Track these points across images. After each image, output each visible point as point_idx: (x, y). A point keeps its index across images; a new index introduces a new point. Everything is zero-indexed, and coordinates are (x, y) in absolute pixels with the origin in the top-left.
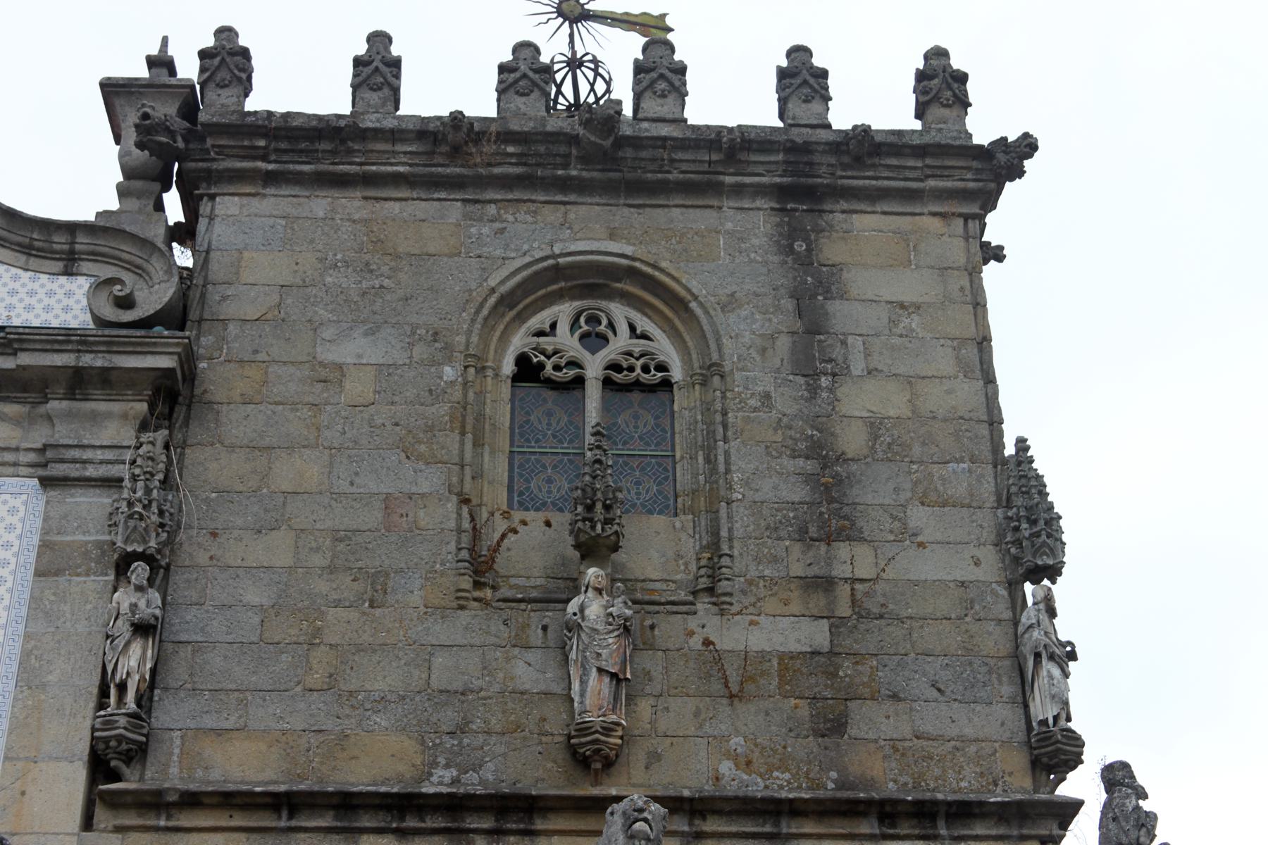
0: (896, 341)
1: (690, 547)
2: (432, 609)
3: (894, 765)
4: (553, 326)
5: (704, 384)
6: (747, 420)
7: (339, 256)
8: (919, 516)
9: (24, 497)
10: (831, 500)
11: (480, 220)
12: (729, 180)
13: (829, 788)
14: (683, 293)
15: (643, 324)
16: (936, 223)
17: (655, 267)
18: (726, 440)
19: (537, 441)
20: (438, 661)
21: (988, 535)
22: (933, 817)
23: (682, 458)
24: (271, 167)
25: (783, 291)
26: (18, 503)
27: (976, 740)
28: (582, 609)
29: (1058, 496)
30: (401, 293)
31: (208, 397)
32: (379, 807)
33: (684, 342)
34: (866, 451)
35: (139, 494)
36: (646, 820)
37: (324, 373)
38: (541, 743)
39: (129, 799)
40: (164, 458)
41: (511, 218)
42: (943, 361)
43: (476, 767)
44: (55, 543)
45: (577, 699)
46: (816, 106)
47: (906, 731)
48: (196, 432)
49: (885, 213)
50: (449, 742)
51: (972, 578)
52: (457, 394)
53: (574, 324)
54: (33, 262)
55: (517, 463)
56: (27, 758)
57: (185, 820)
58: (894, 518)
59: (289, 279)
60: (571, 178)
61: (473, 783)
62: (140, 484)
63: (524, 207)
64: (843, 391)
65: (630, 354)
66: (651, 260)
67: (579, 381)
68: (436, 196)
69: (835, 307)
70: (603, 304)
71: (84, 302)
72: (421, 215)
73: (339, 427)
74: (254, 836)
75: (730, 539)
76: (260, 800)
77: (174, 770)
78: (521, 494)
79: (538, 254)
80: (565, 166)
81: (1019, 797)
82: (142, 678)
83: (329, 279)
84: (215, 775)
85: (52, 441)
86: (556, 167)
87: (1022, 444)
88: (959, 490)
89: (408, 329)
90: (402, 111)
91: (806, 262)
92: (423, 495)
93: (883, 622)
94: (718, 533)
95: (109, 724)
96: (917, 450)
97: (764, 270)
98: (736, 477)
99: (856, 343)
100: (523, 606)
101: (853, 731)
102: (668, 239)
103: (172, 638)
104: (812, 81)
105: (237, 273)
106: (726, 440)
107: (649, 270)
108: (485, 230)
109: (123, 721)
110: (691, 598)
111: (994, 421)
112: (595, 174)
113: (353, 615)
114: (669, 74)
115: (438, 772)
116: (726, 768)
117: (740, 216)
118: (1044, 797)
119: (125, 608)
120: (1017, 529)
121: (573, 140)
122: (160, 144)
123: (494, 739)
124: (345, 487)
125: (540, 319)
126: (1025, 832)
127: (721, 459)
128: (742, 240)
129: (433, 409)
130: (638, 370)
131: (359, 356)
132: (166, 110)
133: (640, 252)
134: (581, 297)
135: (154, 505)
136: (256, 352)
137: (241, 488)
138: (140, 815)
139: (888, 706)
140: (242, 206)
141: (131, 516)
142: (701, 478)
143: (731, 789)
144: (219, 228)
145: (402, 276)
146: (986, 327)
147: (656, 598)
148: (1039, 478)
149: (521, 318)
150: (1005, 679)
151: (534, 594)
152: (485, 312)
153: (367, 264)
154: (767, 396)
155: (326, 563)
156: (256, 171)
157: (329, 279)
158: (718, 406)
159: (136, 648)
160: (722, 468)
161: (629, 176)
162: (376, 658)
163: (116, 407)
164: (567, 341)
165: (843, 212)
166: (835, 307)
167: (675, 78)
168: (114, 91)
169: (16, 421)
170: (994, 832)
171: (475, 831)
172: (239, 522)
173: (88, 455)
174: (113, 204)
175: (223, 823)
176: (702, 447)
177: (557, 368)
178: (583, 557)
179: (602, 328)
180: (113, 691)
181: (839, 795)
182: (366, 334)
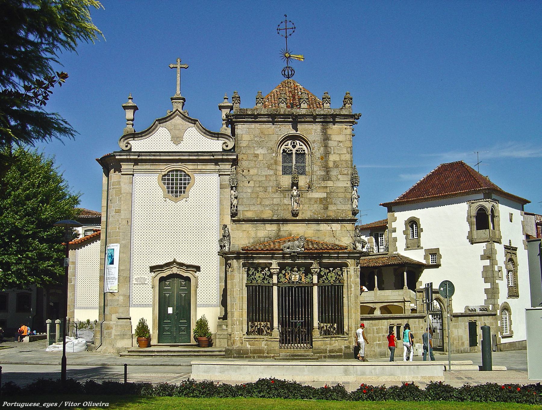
4: (288, 144)
8: (339, 176)
10: (328, 174)
13: (325, 217)
20: (274, 200)
30: (266, 141)
53: (291, 144)
58: (336, 177)
65: (299, 149)
88: (346, 172)
96: (340, 166)
101: (329, 209)
106: (313, 165)
114: (305, 100)
120: (353, 179)
124: (260, 174)
128: (316, 130)
139: (334, 205)
157: (255, 139)
164: (290, 146)
166: (329, 142)
179: (295, 144)
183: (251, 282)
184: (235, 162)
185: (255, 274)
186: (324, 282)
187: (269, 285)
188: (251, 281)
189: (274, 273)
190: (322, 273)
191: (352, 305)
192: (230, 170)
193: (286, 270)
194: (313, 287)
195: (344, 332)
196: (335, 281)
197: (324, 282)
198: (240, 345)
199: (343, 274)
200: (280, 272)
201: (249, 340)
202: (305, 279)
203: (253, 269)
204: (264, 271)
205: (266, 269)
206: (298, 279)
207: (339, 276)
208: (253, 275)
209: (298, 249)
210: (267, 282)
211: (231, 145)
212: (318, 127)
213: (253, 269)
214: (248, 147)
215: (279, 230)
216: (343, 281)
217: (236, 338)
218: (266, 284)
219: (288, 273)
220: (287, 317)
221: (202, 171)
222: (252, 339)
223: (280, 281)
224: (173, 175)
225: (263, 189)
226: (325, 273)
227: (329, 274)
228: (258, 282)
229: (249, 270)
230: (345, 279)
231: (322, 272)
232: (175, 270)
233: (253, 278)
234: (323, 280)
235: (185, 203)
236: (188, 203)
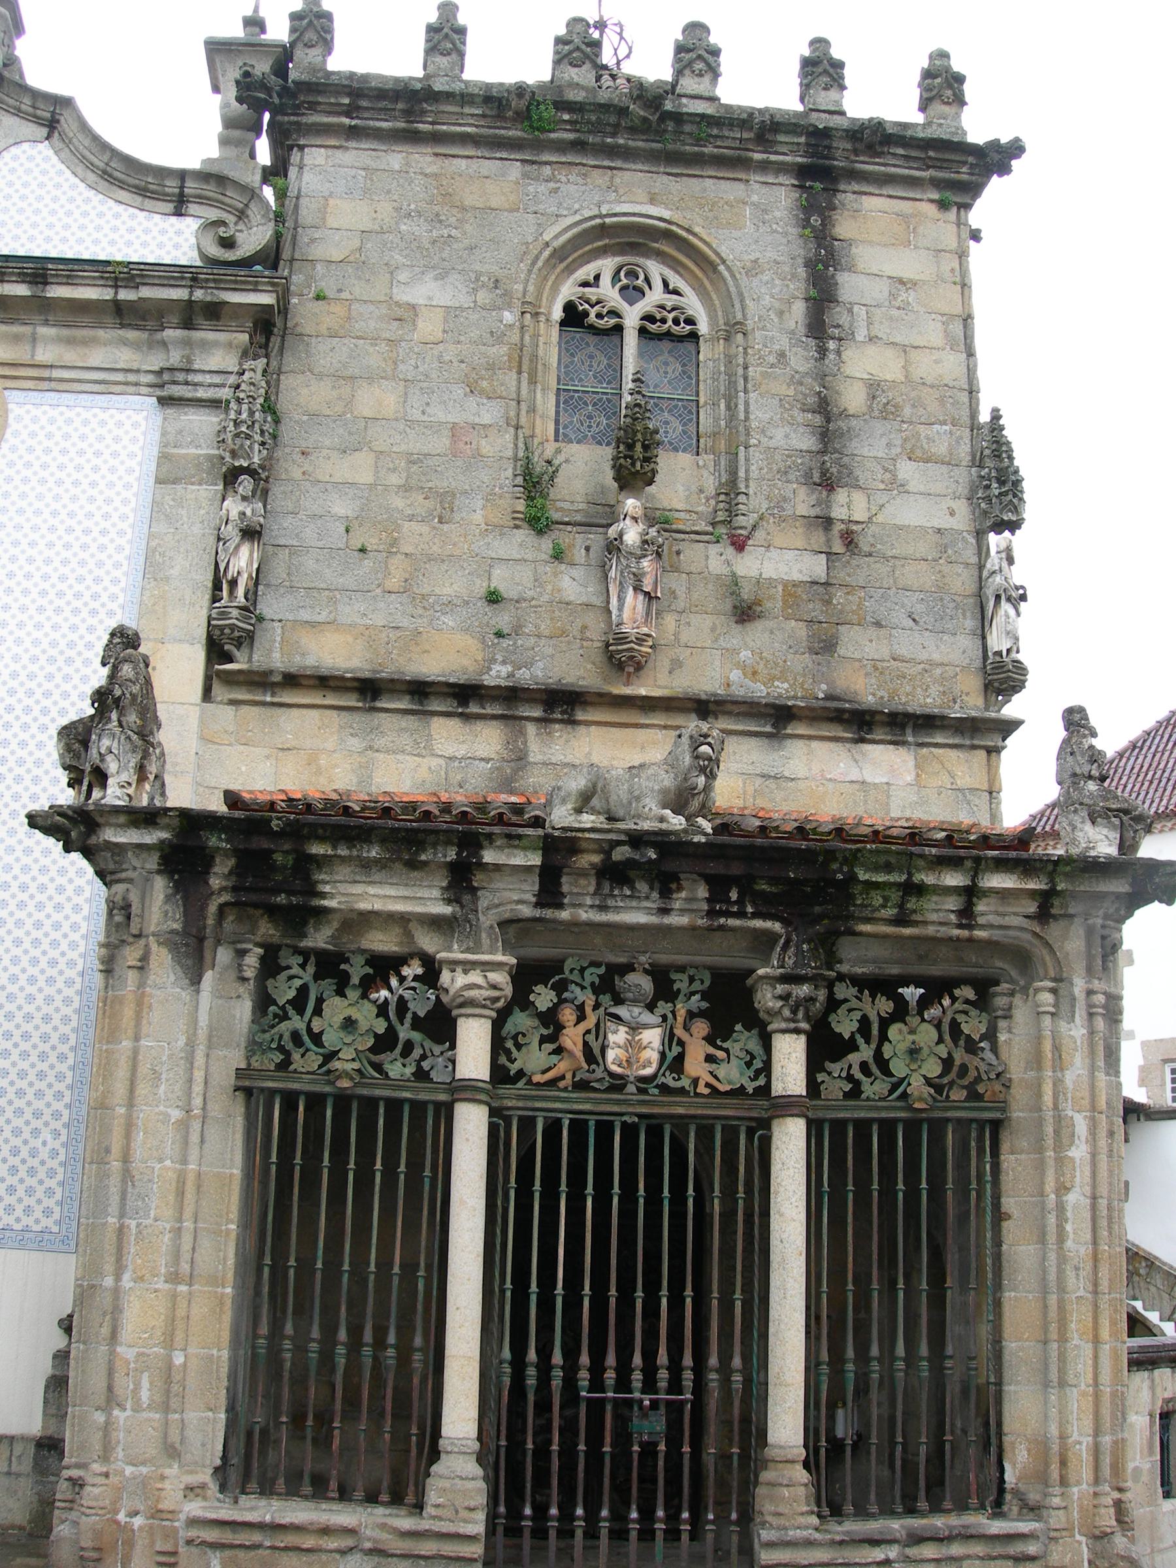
0: (895, 312)
1: (710, 484)
2: (492, 528)
3: (873, 681)
4: (597, 277)
5: (727, 340)
6: (765, 375)
7: (413, 207)
8: (906, 470)
9: (145, 413)
11: (537, 179)
12: (757, 156)
14: (713, 257)
15: (675, 281)
17: (688, 231)
18: (746, 391)
19: (581, 380)
20: (497, 572)
21: (963, 490)
22: (903, 727)
23: (706, 403)
24: (354, 122)
25: (800, 261)
26: (140, 417)
27: (942, 664)
28: (621, 535)
29: (1023, 460)
31: (299, 330)
32: (446, 695)
33: (711, 299)
34: (864, 409)
35: (244, 416)
36: (709, 744)
37: (399, 312)
38: (582, 647)
39: (241, 678)
40: (263, 384)
41: (564, 179)
42: (933, 333)
43: (528, 665)
44: (172, 455)
45: (615, 612)
46: (833, 94)
47: (885, 653)
48: (290, 361)
49: (890, 197)
51: (947, 526)
52: (515, 337)
53: (616, 278)
54: (149, 204)
55: (562, 399)
56: (155, 640)
57: (287, 697)
58: (886, 470)
59: (368, 226)
60: (619, 146)
61: (526, 677)
62: (245, 407)
63: (576, 169)
64: (847, 354)
65: (663, 307)
66: (685, 224)
67: (619, 329)
68: (498, 155)
69: (843, 278)
70: (641, 260)
71: (193, 241)
73: (413, 362)
74: (344, 713)
75: (747, 480)
76: (349, 684)
77: (276, 655)
78: (565, 427)
79: (587, 213)
80: (614, 135)
81: (974, 714)
82: (250, 576)
83: (403, 227)
84: (310, 661)
85: (167, 365)
86: (606, 135)
87: (996, 416)
88: (941, 449)
89: (473, 276)
90: (466, 76)
92: (484, 426)
93: (871, 559)
94: (736, 473)
96: (907, 411)
97: (784, 241)
98: (754, 424)
100: (569, 528)
101: (841, 650)
102: (702, 207)
103: (272, 541)
104: (831, 71)
105: (324, 219)
107: (684, 234)
108: (543, 188)
109: (235, 613)
110: (710, 529)
111: (972, 391)
112: (640, 144)
113: (425, 529)
114: (706, 55)
115: (496, 667)
116: (735, 675)
117: (765, 190)
118: (993, 715)
119: (234, 515)
120: (988, 487)
121: (623, 111)
122: (258, 99)
123: (543, 642)
124: (416, 414)
125: (586, 272)
126: (976, 742)
127: (741, 407)
128: (765, 211)
129: (494, 349)
130: (670, 323)
131: (430, 298)
132: (262, 67)
133: (676, 217)
134: (622, 253)
135: (257, 426)
136: (340, 291)
137: (328, 412)
138: (249, 692)
139: (872, 632)
140: (328, 157)
141: (237, 435)
142: (723, 423)
143: (739, 692)
144: (307, 176)
145: (468, 228)
146: (970, 306)
147: (681, 527)
148: (1008, 443)
149: (570, 270)
150: (968, 614)
151: (579, 518)
152: (540, 263)
153: (437, 215)
154: (782, 355)
155: (402, 482)
156: (341, 126)
157: (403, 227)
158: (741, 361)
159: (245, 550)
160: (742, 416)
161: (670, 147)
162: (444, 567)
163: (222, 337)
164: (608, 292)
165: (854, 193)
167: (710, 59)
168: (217, 50)
169: (136, 346)
170: (950, 741)
171: (527, 719)
172: (327, 442)
174: (214, 151)
175: (319, 701)
176: (724, 396)
177: (599, 316)
178: (621, 488)
179: (640, 282)
180: (225, 586)
181: (829, 704)
182: (436, 279)
183: (284, 1065)
185: (320, 1001)
186: (855, 1092)
187: (423, 1096)
188: (278, 1057)
189: (471, 1003)
190: (845, 1025)
191: (1070, 1273)
194: (766, 1124)
195: (1001, 1490)
196: (939, 1089)
197: (855, 1092)
199: (1002, 1037)
200: (521, 999)
202: (710, 1059)
203: (303, 966)
204: (394, 982)
205: (406, 971)
206: (655, 1056)
207: (972, 1047)
208: (301, 1012)
210: (409, 1071)
213: (303, 966)
214: (357, 263)
215: (520, 759)
216: (998, 1087)
217: (121, 1517)
218: (399, 1084)
219: (581, 1008)
220: (557, 1358)
221: (56, 374)
222: (256, 1537)
223: (514, 1068)
225: (430, 504)
226: (865, 1022)
227: (894, 1031)
228: (336, 1065)
230: (1017, 1071)
231: (842, 1011)
233: (296, 1037)
234: (850, 1078)
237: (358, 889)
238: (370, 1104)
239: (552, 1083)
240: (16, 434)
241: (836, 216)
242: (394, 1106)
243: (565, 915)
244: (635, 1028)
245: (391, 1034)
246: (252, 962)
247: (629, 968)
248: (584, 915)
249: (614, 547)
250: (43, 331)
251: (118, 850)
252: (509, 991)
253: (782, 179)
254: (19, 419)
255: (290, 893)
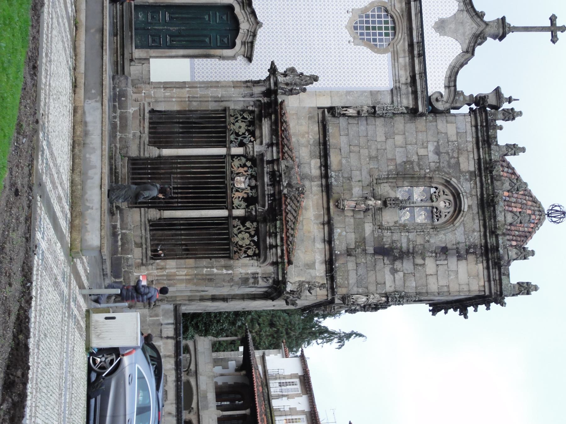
4: (446, 195)
8: (401, 274)
16: (482, 283)
20: (358, 172)
21: (398, 289)
26: (387, 85)
28: (371, 200)
37: (425, 144)
43: (336, 181)
50: (340, 175)
64: (432, 259)
65: (440, 212)
72: (470, 162)
91: (467, 252)
95: (338, 109)
99: (446, 262)
108: (467, 177)
113: (367, 154)
125: (447, 191)
149: (446, 186)
159: (355, 112)
166: (455, 259)
173: (399, 97)
183: (231, 116)
184: (413, 112)
185: (245, 122)
187: (227, 142)
189: (246, 148)
190: (248, 224)
192: (400, 105)
193: (251, 167)
194: (227, 209)
197: (234, 227)
198: (134, 98)
199: (248, 258)
201: (141, 111)
202: (239, 197)
206: (239, 187)
209: (285, 181)
210: (232, 140)
211: (440, 106)
212: (476, 237)
215: (311, 179)
216: (237, 257)
217: (144, 91)
220: (178, 170)
222: (142, 115)
224: (386, 22)
226: (248, 228)
227: (247, 234)
228: (232, 125)
229: (252, 112)
232: (244, 26)
233: (237, 118)
234: (237, 226)
235: (346, 41)
236: (347, 45)
237: (267, 126)
238: (225, 132)
239: (232, 167)
240: (379, 57)
241: (474, 256)
242: (225, 137)
243: (265, 166)
244: (244, 182)
245: (239, 136)
246: (251, 108)
247: (256, 181)
248: (265, 169)
249: (366, 198)
250: (407, 59)
251: (270, 80)
252: (249, 157)
253: (483, 241)
254: (384, 57)
255: (265, 113)
